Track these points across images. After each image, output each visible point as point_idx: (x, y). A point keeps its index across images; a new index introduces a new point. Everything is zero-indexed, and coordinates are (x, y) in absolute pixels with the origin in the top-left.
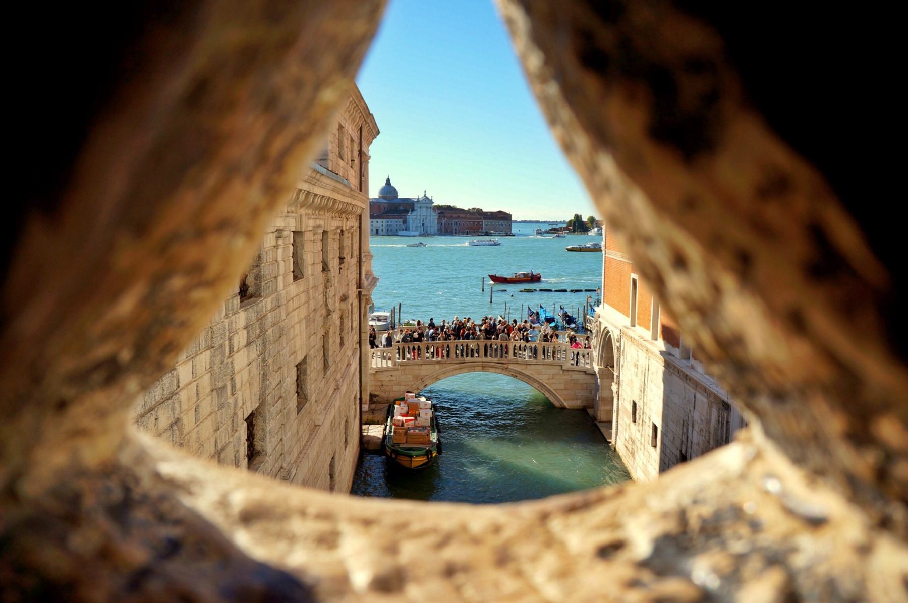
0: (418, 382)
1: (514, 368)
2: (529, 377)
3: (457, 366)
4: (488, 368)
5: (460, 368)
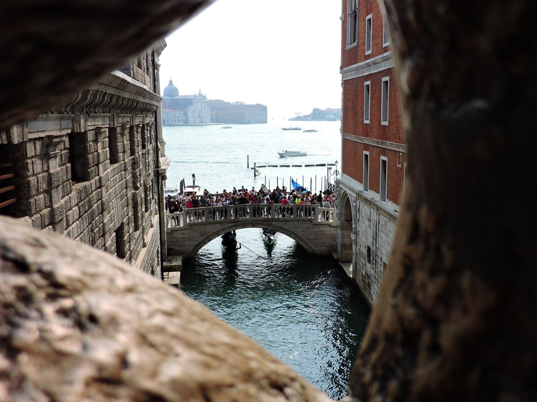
1: (277, 224)
3: (233, 224)
4: (257, 225)
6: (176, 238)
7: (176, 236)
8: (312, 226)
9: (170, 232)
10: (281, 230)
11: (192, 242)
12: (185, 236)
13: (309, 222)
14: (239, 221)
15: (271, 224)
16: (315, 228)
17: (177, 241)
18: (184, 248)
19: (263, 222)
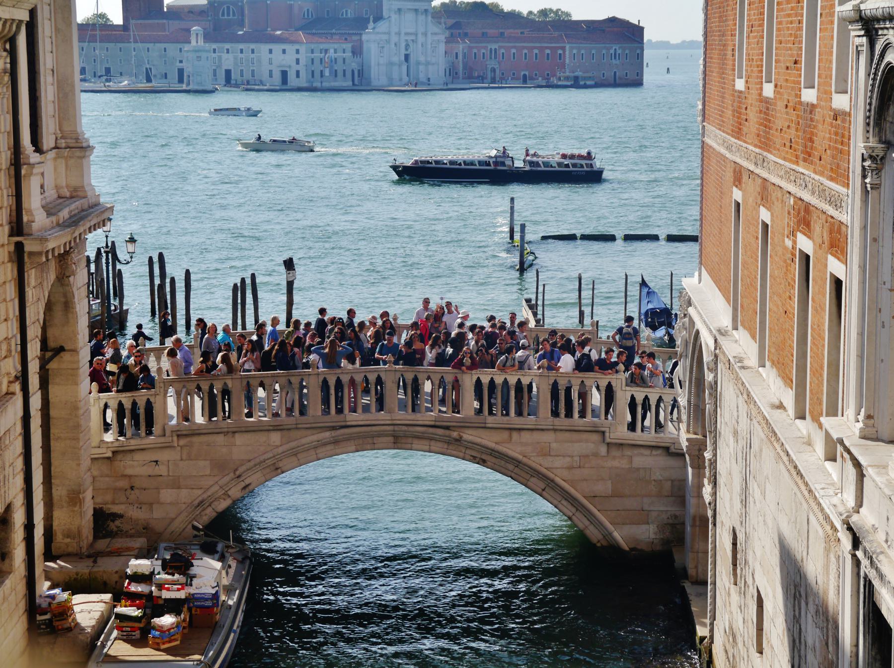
0: (227, 479)
1: (478, 440)
2: (517, 463)
3: (327, 434)
4: (410, 440)
5: (336, 442)
6: (130, 476)
7: (129, 472)
8: (603, 450)
9: (109, 454)
10: (494, 460)
11: (184, 492)
12: (162, 470)
13: (596, 437)
14: (349, 423)
15: (458, 437)
16: (614, 458)
17: (132, 488)
18: (158, 513)
19: (431, 430)
